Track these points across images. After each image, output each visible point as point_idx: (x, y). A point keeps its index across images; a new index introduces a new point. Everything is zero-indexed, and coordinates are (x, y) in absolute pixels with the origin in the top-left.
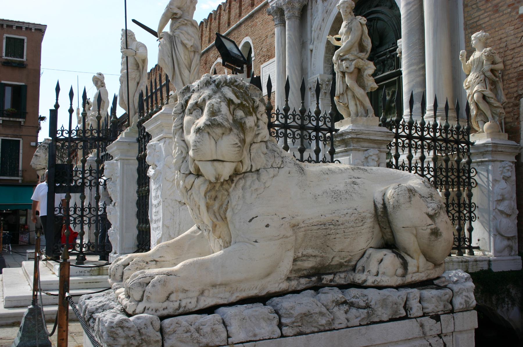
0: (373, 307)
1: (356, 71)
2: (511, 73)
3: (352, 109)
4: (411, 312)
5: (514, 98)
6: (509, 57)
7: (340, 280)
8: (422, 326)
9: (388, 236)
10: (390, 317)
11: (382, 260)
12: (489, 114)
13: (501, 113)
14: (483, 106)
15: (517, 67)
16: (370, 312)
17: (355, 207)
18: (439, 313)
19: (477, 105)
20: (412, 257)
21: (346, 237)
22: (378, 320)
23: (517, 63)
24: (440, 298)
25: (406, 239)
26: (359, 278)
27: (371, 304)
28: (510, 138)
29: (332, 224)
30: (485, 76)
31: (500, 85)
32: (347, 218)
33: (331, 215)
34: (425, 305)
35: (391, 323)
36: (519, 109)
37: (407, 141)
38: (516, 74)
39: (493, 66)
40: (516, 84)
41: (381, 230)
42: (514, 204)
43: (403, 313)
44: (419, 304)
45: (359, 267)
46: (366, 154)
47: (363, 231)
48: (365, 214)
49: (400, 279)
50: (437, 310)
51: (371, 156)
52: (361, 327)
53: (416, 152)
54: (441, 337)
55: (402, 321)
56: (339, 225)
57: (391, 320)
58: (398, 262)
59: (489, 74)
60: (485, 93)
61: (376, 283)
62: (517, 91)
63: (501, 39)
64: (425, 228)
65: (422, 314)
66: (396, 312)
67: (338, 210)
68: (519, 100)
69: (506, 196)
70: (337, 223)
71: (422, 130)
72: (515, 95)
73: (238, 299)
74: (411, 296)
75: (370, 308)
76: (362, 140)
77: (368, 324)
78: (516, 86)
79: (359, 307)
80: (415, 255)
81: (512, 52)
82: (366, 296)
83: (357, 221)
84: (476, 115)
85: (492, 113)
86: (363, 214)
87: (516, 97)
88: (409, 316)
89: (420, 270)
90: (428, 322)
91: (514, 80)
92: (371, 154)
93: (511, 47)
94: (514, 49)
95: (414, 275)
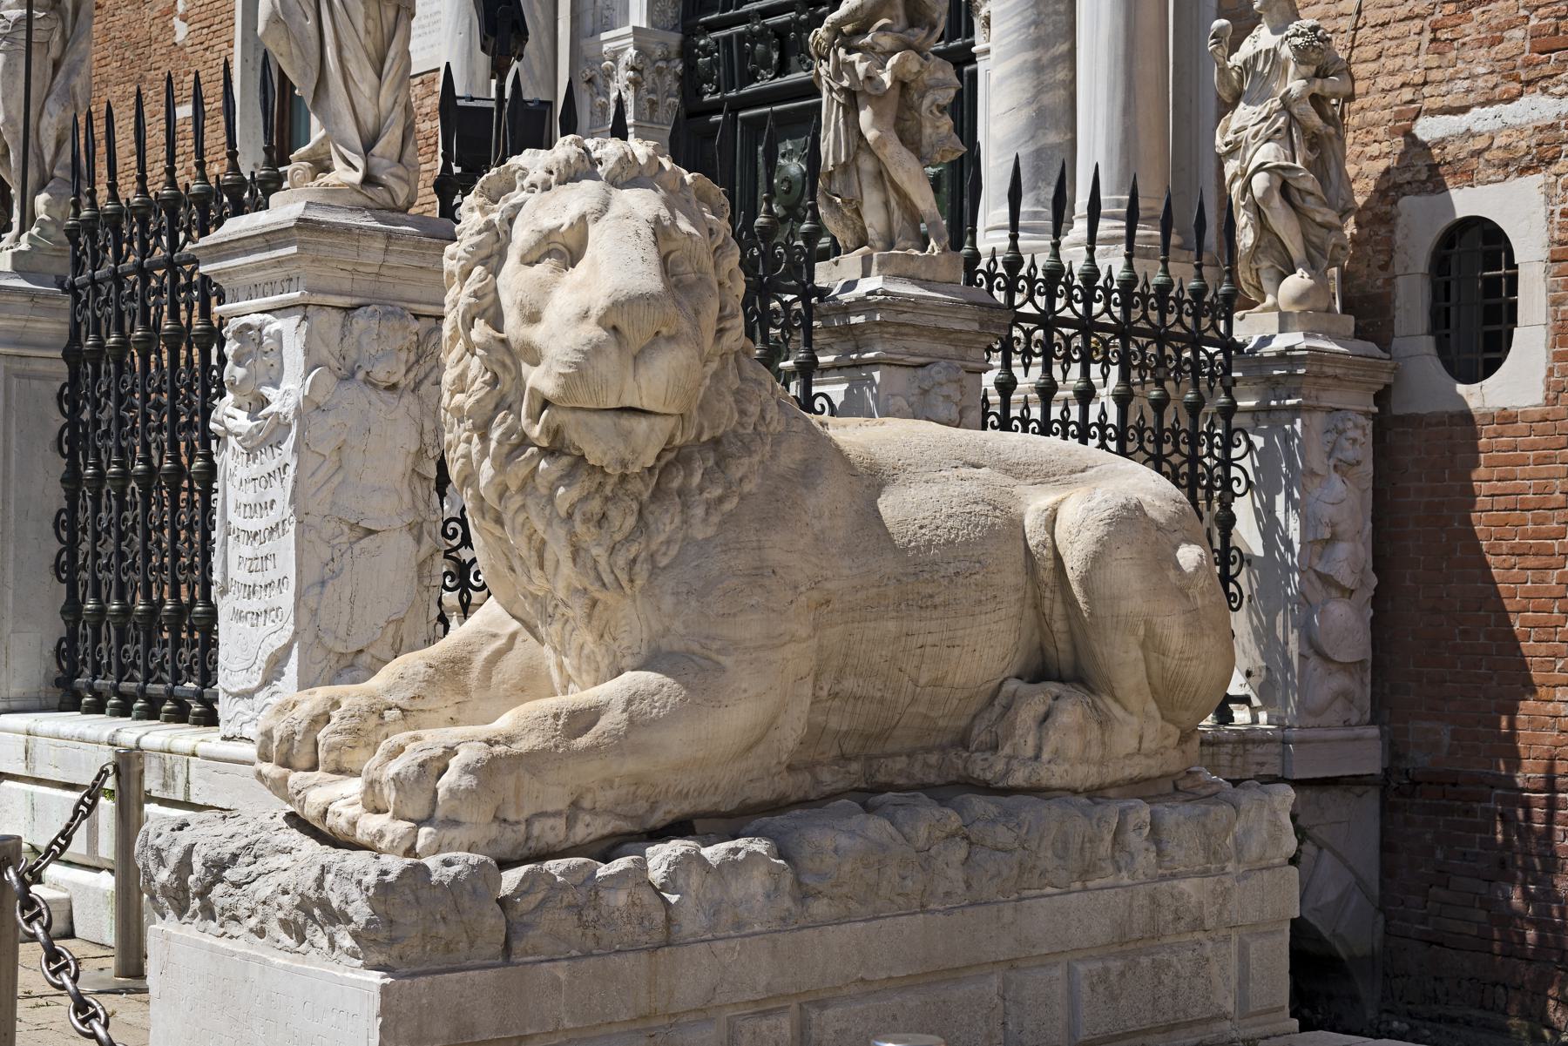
1: (898, 87)
2: (1371, 108)
3: (874, 220)
6: (1369, 51)
12: (1296, 249)
14: (1283, 223)
20: (1125, 709)
23: (1392, 74)
36: (1392, 231)
37: (1039, 334)
38: (1387, 114)
39: (1317, 85)
42: (1365, 555)
53: (1027, 367)
60: (1286, 175)
68: (1395, 202)
69: (1340, 529)
71: (1088, 301)
73: (670, 818)
81: (1378, 35)
84: (1256, 246)
85: (1307, 241)
91: (1380, 132)
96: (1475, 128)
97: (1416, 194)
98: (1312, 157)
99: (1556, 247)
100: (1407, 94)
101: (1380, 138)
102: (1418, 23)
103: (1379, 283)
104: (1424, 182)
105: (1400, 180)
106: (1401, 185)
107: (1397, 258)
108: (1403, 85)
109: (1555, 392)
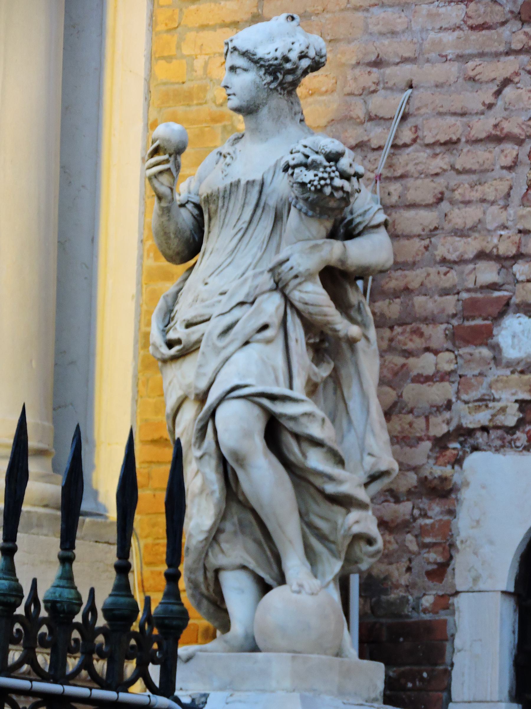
5: (427, 445)
6: (421, 190)
13: (358, 538)
15: (461, 261)
19: (228, 471)
23: (461, 233)
30: (287, 301)
31: (369, 363)
36: (452, 513)
38: (450, 304)
40: (445, 362)
59: (313, 294)
60: (279, 408)
62: (449, 406)
63: (378, 63)
68: (458, 461)
72: (439, 428)
78: (443, 377)
87: (440, 443)
91: (437, 334)
93: (437, 129)
94: (450, 144)
97: (497, 450)
98: (324, 372)
100: (488, 273)
101: (434, 345)
102: (510, 150)
103: (427, 601)
104: (511, 430)
106: (470, 432)
107: (461, 562)
108: (482, 255)
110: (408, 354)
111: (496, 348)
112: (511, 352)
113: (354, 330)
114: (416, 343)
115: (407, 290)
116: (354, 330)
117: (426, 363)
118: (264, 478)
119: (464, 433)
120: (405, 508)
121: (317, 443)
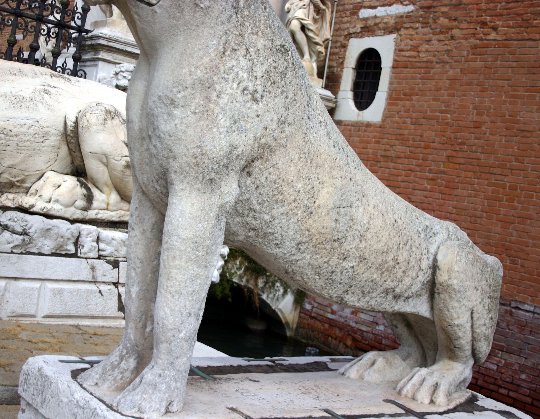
0: (31, 234)
4: (82, 251)
7: (7, 201)
8: (93, 268)
9: (78, 162)
10: (53, 251)
11: (59, 186)
16: (26, 239)
17: (38, 118)
18: (119, 259)
20: (101, 191)
21: (18, 151)
22: (36, 252)
24: (124, 242)
25: (94, 167)
26: (26, 201)
27: (30, 231)
28: (326, 87)
29: (3, 133)
32: (24, 129)
33: (3, 123)
34: (102, 246)
35: (53, 257)
36: (345, 51)
38: (351, 6)
40: (349, 19)
41: (70, 154)
43: (71, 248)
44: (95, 244)
45: (32, 190)
46: (117, 68)
47: (44, 149)
48: (49, 129)
49: (79, 212)
50: (118, 255)
51: (123, 72)
52: (11, 255)
54: (117, 287)
55: (67, 258)
56: (12, 136)
57: (53, 254)
58: (80, 191)
60: (304, 22)
61: (45, 210)
62: (348, 28)
64: (119, 158)
65: (97, 256)
66: (62, 246)
67: (14, 118)
68: (348, 40)
70: (10, 133)
72: (346, 33)
74: (84, 233)
75: (27, 235)
76: (115, 50)
77: (22, 253)
78: (348, 22)
79: (14, 232)
80: (105, 189)
82: (26, 221)
83: (36, 136)
86: (46, 129)
87: (346, 36)
88: (79, 255)
89: (110, 207)
90: (103, 267)
91: (348, 13)
92: (123, 69)
95: (102, 212)
96: (379, 14)
99: (395, 63)
104: (358, 33)
105: (351, 32)
109: (385, 117)
110: (343, 17)
111: (358, 16)
112: (361, 17)
113: (324, 7)
114: (344, 15)
115: (344, 4)
116: (324, 7)
117: (345, 19)
118: (300, 37)
119: (350, 34)
120: (337, 50)
121: (312, 31)
